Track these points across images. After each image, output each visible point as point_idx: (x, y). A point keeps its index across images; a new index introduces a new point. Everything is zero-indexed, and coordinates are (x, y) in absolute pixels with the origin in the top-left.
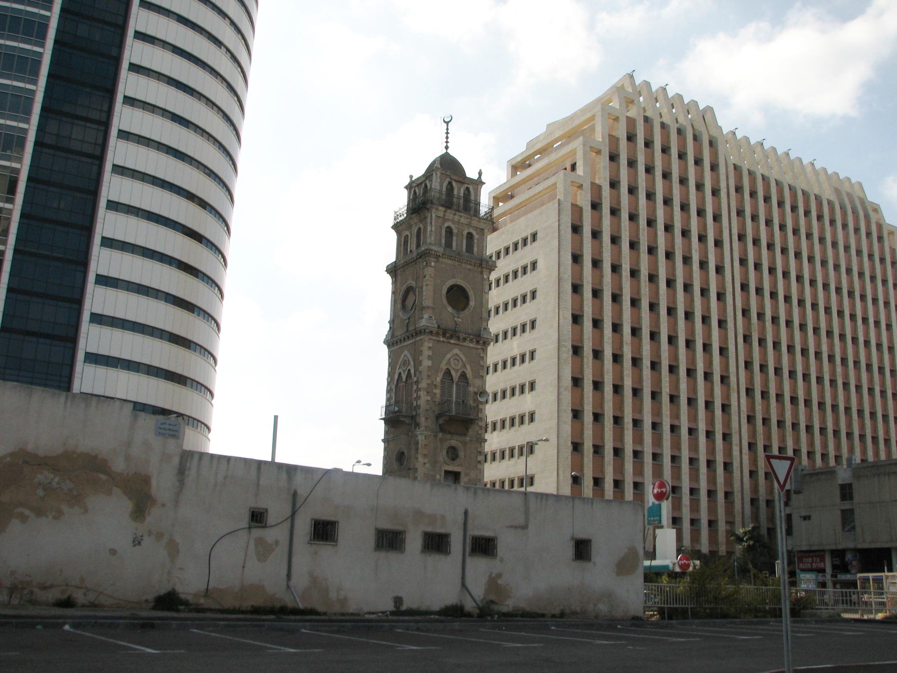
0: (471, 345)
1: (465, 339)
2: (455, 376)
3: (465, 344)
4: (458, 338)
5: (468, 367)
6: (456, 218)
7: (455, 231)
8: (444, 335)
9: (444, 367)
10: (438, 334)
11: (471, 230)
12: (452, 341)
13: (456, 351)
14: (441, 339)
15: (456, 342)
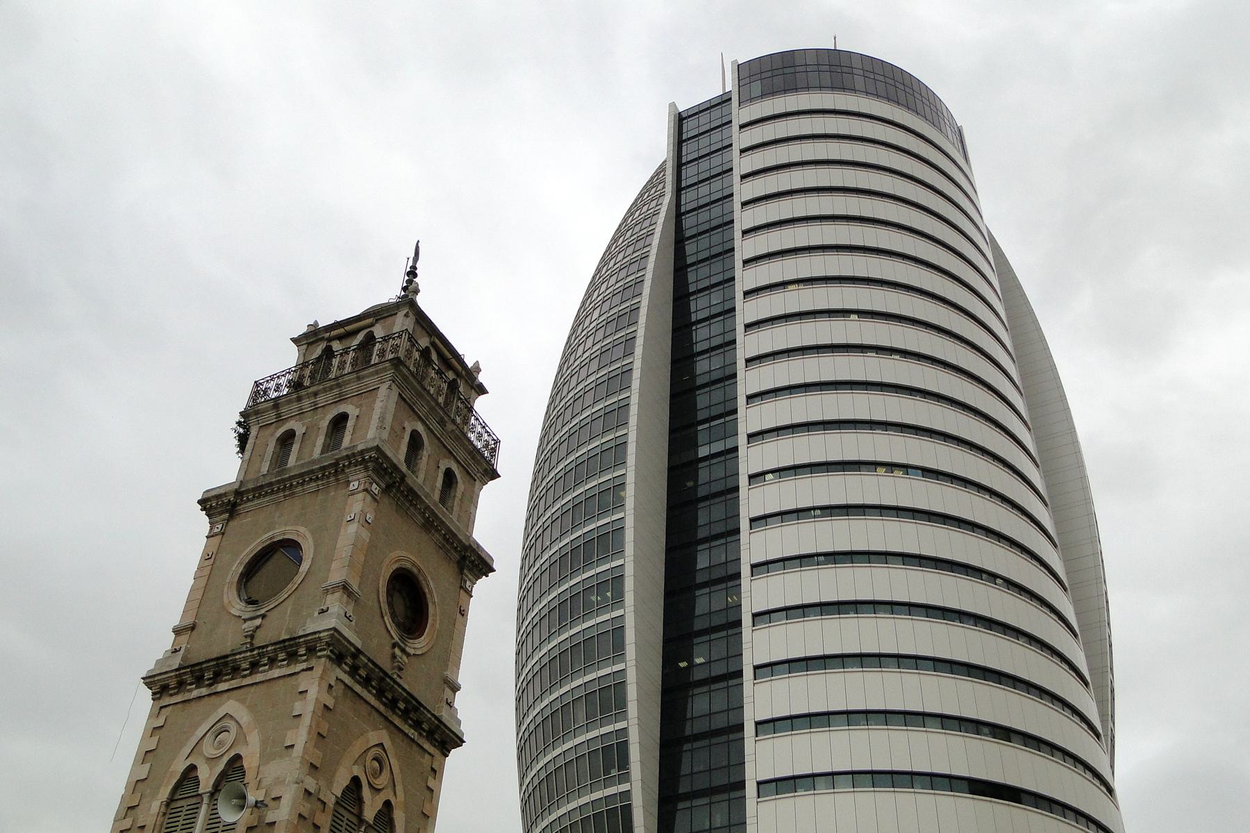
0: (276, 673)
1: (254, 666)
2: (207, 776)
3: (259, 677)
4: (236, 670)
5: (254, 739)
6: (306, 403)
7: (299, 433)
8: (199, 681)
9: (180, 766)
10: (181, 685)
11: (342, 408)
12: (222, 687)
13: (231, 706)
14: (195, 693)
15: (235, 683)
